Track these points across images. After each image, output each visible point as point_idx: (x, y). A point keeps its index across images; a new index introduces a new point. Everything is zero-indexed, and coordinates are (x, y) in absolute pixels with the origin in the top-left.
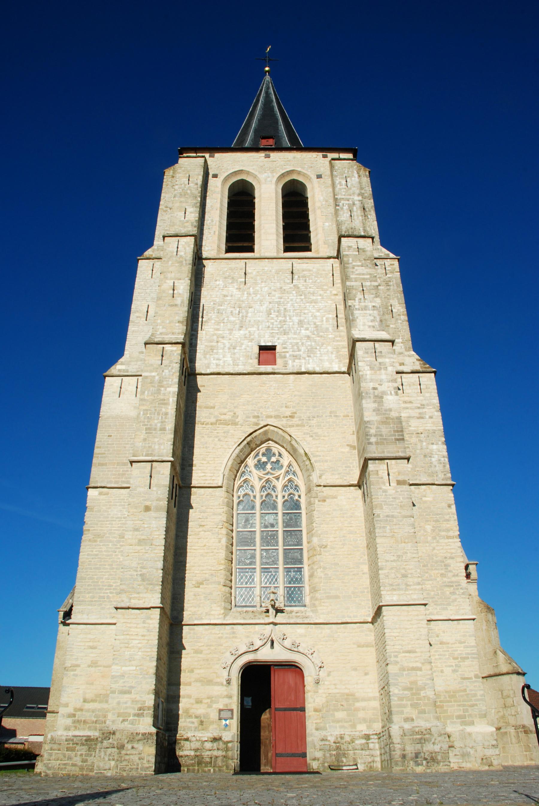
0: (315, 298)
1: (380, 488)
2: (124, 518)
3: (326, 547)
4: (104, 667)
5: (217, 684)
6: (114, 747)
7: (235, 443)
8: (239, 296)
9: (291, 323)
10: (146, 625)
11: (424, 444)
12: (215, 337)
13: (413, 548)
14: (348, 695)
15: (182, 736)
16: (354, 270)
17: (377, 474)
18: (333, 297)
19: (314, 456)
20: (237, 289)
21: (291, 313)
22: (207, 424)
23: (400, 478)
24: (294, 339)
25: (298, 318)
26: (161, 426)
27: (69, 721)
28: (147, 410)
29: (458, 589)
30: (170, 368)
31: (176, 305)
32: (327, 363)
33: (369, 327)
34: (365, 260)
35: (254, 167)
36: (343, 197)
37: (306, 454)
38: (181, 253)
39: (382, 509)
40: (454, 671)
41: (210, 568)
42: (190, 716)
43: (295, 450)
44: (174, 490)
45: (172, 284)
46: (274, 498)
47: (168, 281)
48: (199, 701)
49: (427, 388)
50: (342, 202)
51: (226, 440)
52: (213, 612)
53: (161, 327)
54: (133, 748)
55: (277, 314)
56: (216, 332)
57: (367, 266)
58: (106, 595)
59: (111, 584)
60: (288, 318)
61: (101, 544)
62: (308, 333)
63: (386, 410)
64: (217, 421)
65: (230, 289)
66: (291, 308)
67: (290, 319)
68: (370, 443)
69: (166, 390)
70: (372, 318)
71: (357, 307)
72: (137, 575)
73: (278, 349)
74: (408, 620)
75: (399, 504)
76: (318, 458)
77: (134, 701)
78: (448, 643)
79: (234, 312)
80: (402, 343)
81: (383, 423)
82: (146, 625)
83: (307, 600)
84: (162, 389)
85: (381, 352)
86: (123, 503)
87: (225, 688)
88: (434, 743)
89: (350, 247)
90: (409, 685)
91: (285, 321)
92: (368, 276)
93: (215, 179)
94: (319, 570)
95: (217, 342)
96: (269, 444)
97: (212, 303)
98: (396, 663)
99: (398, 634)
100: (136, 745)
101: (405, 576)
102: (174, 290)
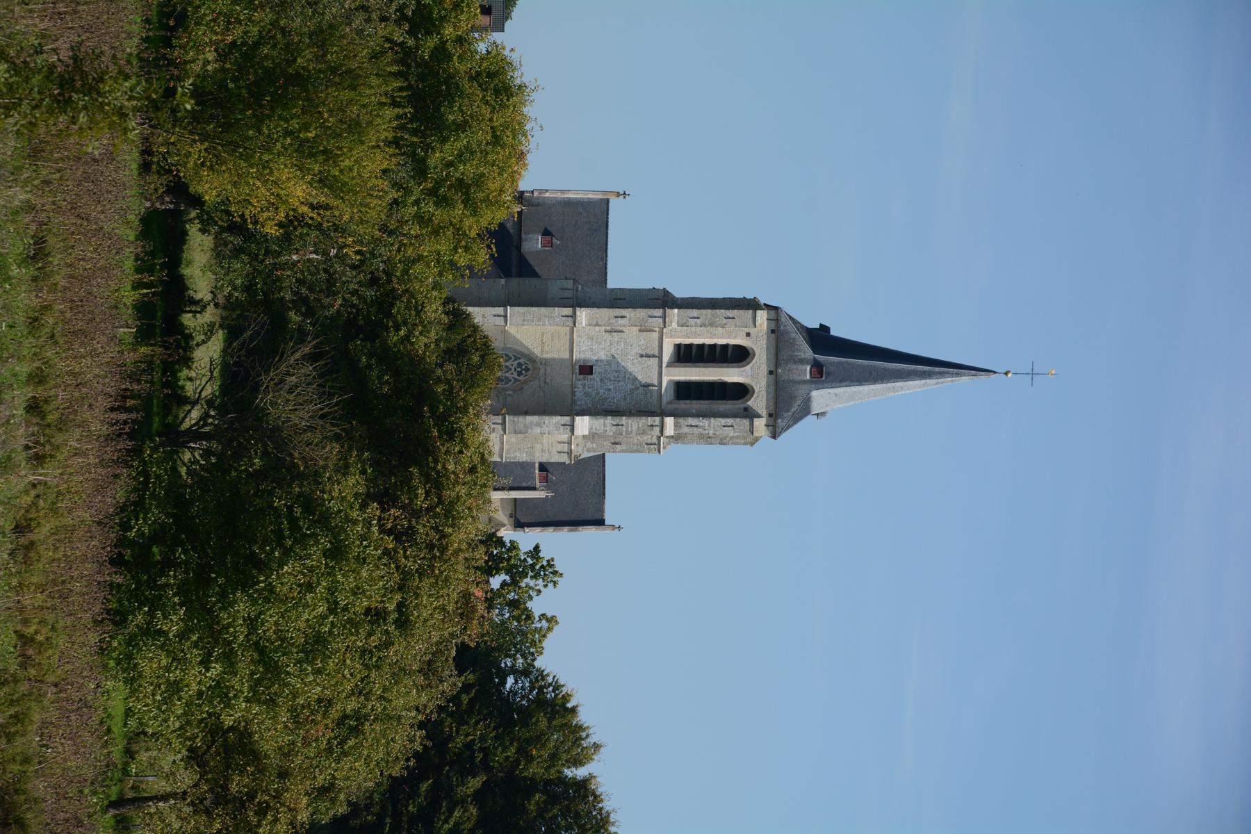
38: (651, 320)
62: (601, 394)
73: (590, 376)
81: (525, 425)
89: (654, 421)
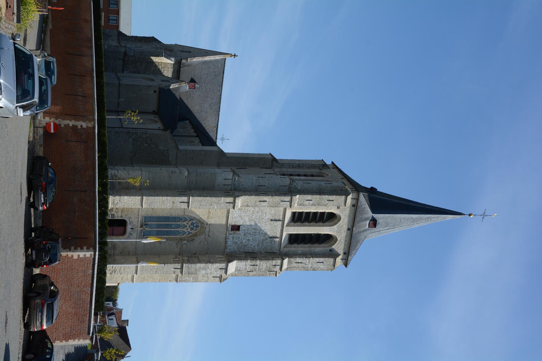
0: (260, 245)
9: (249, 237)
12: (246, 211)
16: (265, 263)
21: (254, 237)
24: (242, 238)
25: (251, 239)
32: (229, 248)
33: (238, 266)
34: (270, 267)
35: (342, 223)
36: (311, 261)
38: (282, 203)
50: (308, 260)
52: (143, 212)
55: (254, 232)
57: (266, 268)
62: (244, 242)
63: (200, 270)
66: (256, 237)
67: (251, 236)
70: (241, 267)
71: (247, 263)
73: (238, 232)
80: (235, 273)
84: (216, 204)
87: (120, 216)
89: (277, 263)
91: (250, 234)
92: (261, 268)
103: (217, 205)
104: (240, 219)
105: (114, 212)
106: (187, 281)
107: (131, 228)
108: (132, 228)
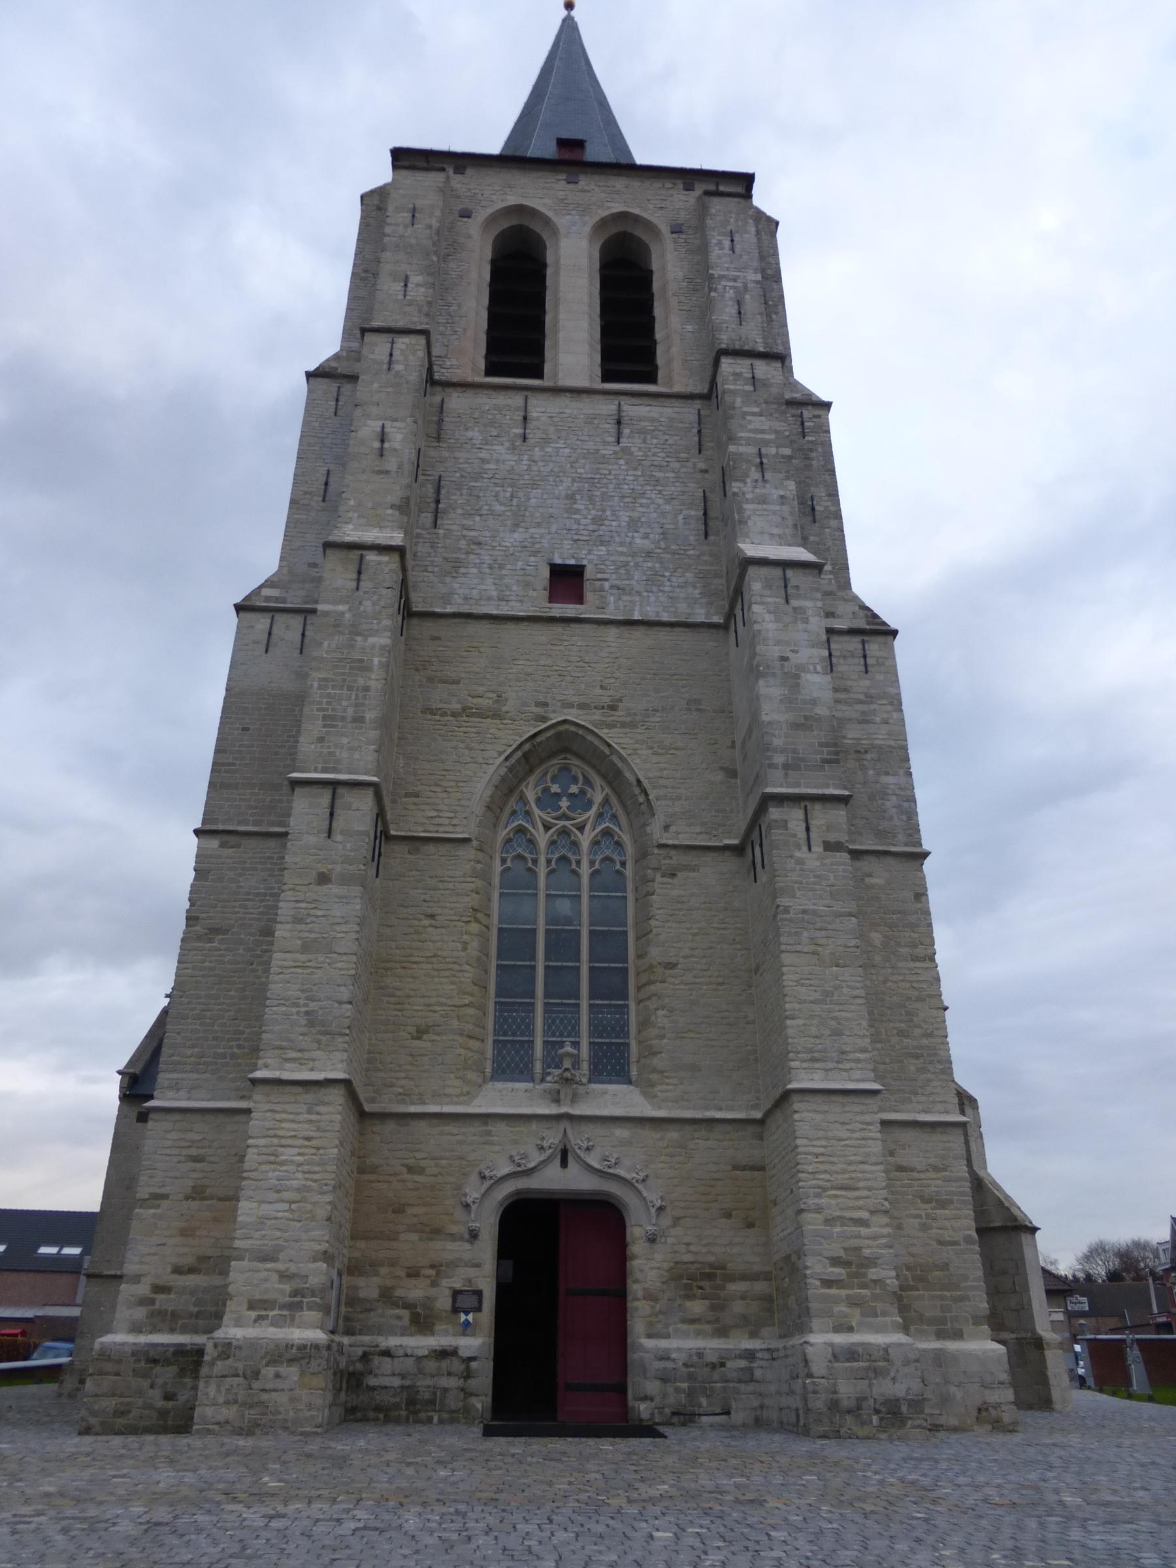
1: (791, 857)
2: (272, 895)
3: (672, 966)
4: (220, 1199)
5: (453, 1237)
6: (237, 1375)
7: (500, 754)
8: (513, 463)
10: (313, 1117)
11: (871, 772)
12: (463, 544)
13: (854, 979)
14: (712, 1266)
15: (377, 1346)
17: (785, 827)
18: (699, 476)
19: (654, 788)
20: (508, 449)
22: (444, 714)
23: (832, 837)
26: (355, 712)
27: (140, 1313)
28: (325, 680)
29: (931, 1063)
30: (375, 598)
31: (387, 472)
34: (766, 402)
37: (639, 782)
38: (398, 367)
39: (794, 896)
40: (924, 1227)
41: (444, 1000)
42: (395, 1305)
43: (619, 773)
44: (378, 841)
45: (379, 429)
46: (574, 866)
47: (369, 422)
48: (413, 1273)
49: (878, 664)
50: (723, 283)
51: (482, 747)
52: (448, 1091)
53: (356, 515)
54: (277, 1376)
56: (465, 532)
57: (771, 415)
58: (230, 1051)
59: (241, 1028)
60: (608, 513)
61: (223, 947)
62: (647, 544)
64: (464, 709)
65: (495, 447)
68: (771, 766)
69: (365, 641)
71: (749, 496)
72: (298, 1013)
73: (589, 573)
74: (844, 1123)
75: (828, 889)
76: (662, 792)
77: (284, 1276)
78: (912, 1170)
79: (502, 494)
82: (313, 1117)
83: (634, 1072)
84: (359, 638)
85: (797, 587)
86: (269, 866)
87: (467, 1246)
88: (894, 1379)
89: (737, 375)
90: (842, 1253)
92: (772, 437)
93: (466, 219)
94: (660, 1013)
95: (467, 553)
96: (565, 758)
97: (458, 475)
98: (819, 1210)
99: (822, 1150)
100: (283, 1370)
101: (837, 1033)
102: (382, 441)
103: (366, 637)
104: (509, 567)
105: (433, 1292)
106: (906, 804)
107: (564, 1163)
108: (557, 1161)
